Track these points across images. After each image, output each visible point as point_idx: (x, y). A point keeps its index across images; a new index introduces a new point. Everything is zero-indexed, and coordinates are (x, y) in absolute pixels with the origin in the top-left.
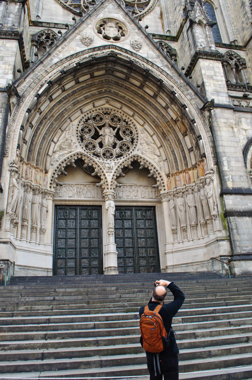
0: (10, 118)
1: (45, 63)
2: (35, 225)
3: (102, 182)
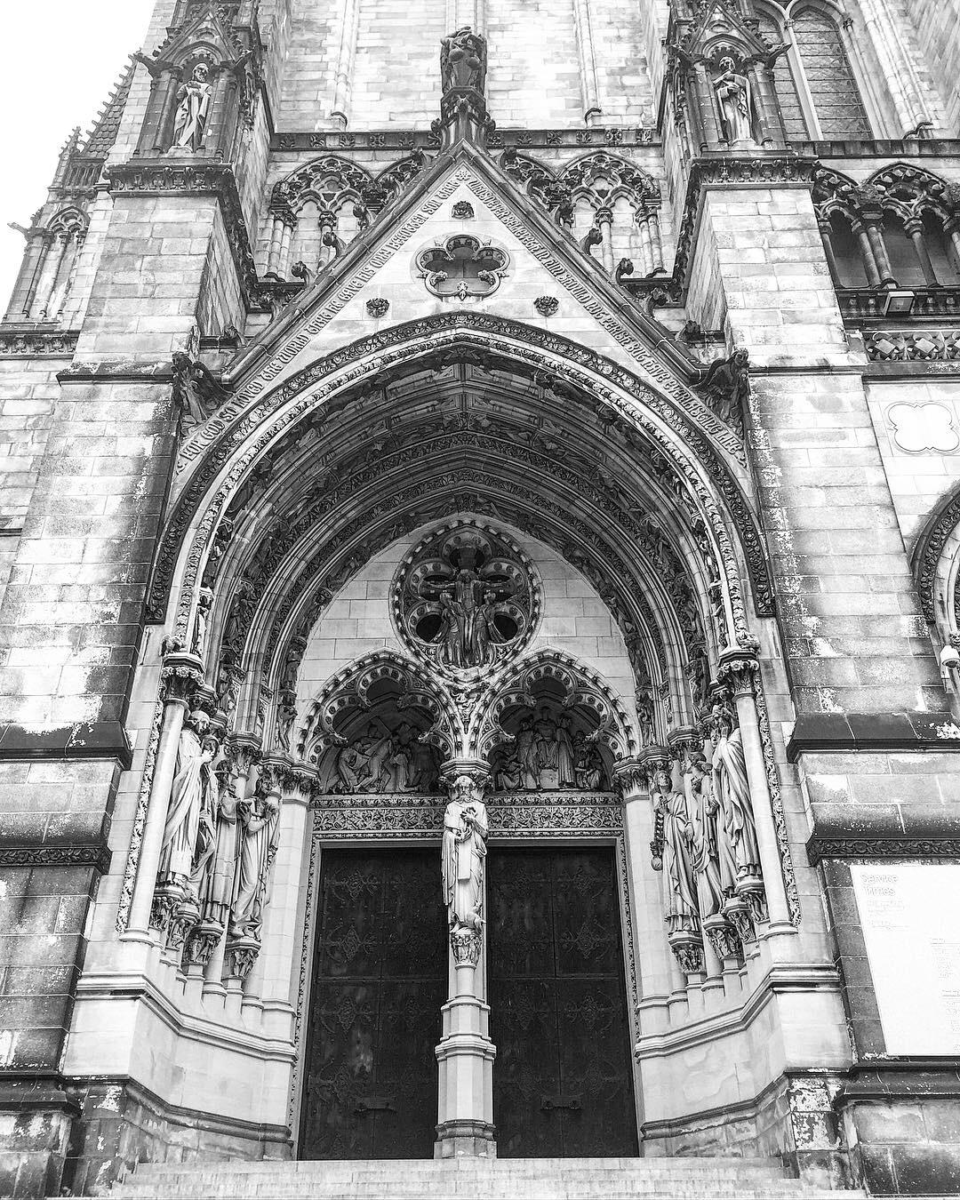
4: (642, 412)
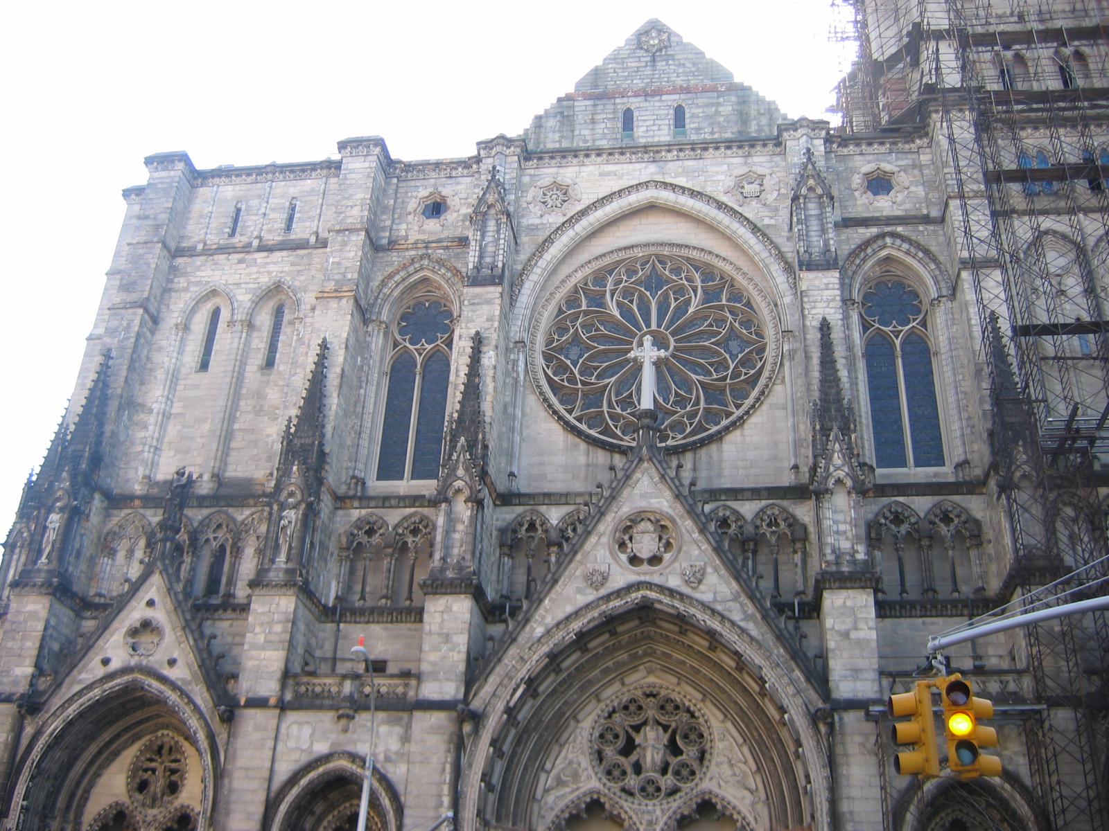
0: (464, 760)
1: (520, 639)
4: (194, 723)
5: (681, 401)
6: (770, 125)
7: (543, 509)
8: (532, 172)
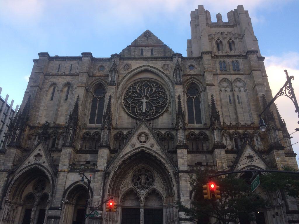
0: (106, 182)
2: (114, 220)
3: (140, 200)
5: (151, 110)
6: (170, 54)
7: (123, 131)
8: (122, 62)
